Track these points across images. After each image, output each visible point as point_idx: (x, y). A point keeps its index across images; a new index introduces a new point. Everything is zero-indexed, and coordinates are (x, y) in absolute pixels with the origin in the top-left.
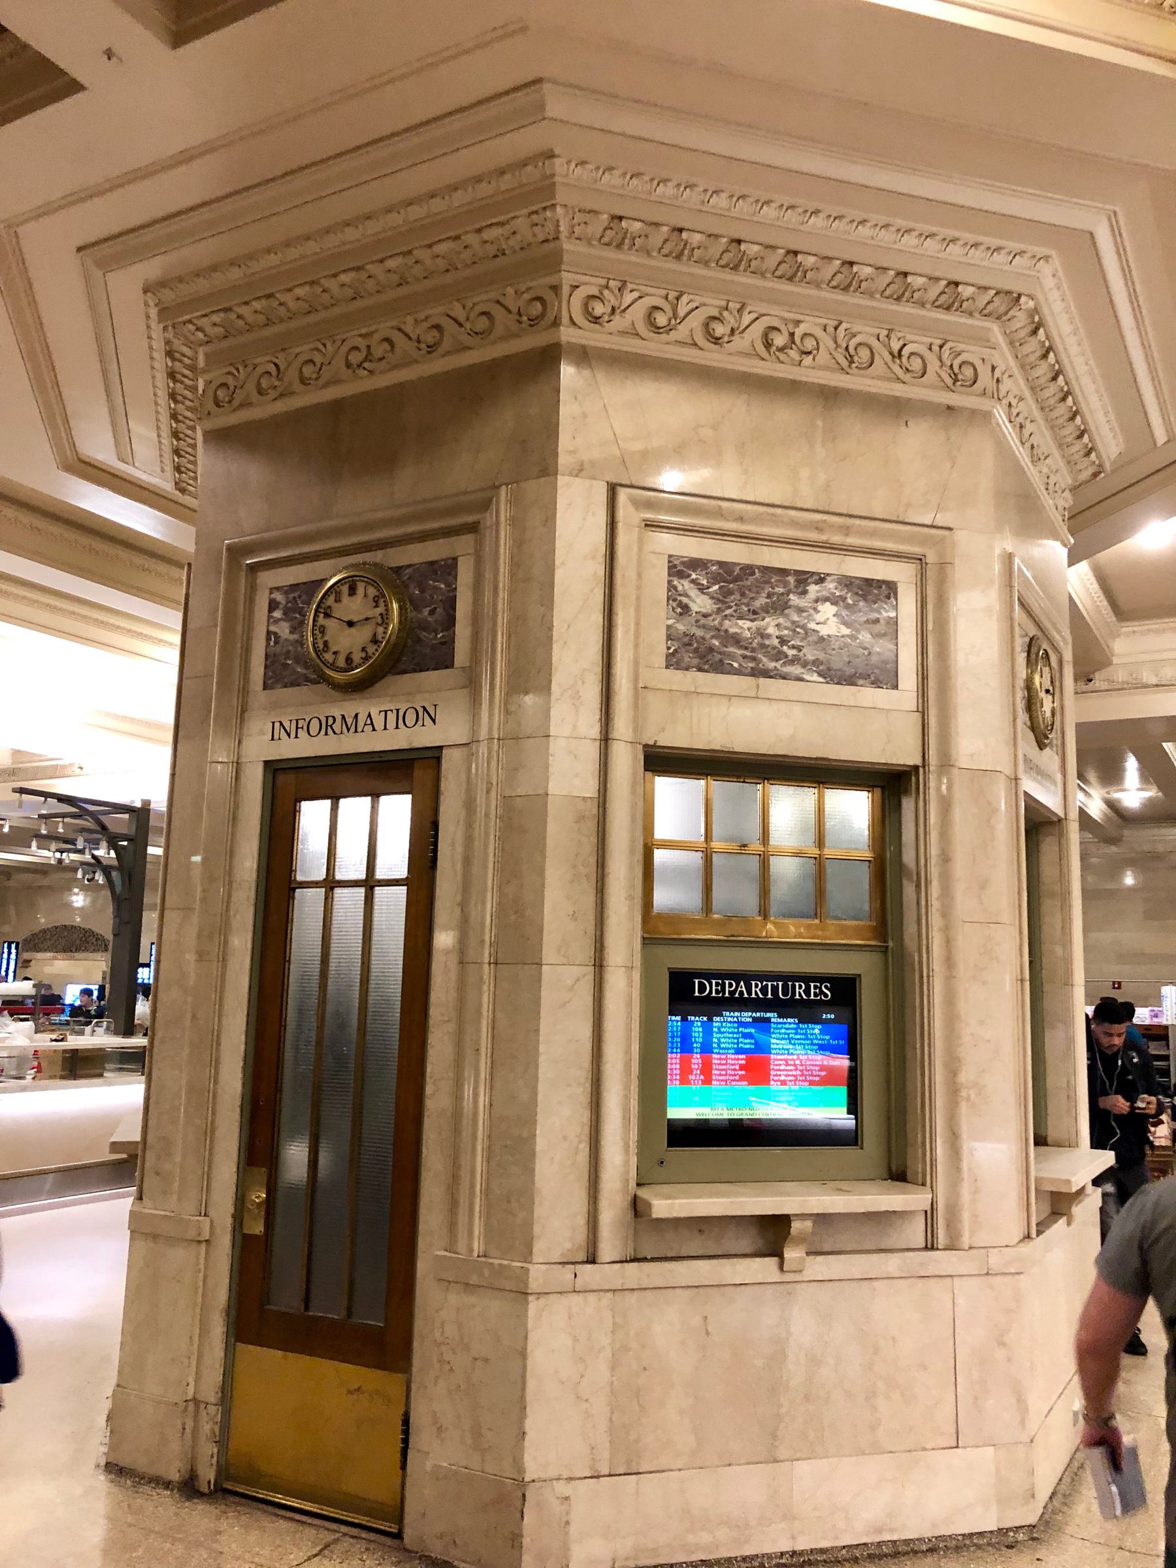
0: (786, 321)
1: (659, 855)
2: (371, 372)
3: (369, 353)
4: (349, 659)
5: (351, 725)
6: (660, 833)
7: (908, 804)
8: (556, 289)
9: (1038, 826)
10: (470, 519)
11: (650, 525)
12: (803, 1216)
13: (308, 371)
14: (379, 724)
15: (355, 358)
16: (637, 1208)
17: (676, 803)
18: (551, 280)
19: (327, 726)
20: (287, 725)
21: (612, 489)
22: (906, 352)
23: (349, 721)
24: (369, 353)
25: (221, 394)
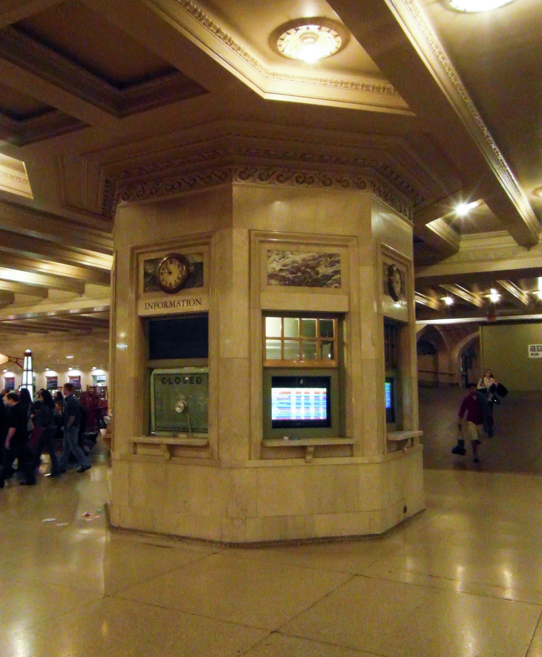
0: (304, 174)
1: (268, 341)
2: (174, 193)
3: (173, 186)
4: (170, 284)
5: (172, 305)
6: (268, 334)
7: (345, 323)
8: (230, 170)
9: (393, 328)
10: (206, 240)
11: (262, 242)
12: (311, 446)
13: (154, 191)
14: (181, 303)
15: (168, 187)
16: (263, 445)
17: (273, 326)
18: (230, 167)
19: (165, 305)
20: (151, 305)
21: (250, 232)
22: (342, 180)
23: (172, 303)
24: (173, 186)
25: (125, 196)
